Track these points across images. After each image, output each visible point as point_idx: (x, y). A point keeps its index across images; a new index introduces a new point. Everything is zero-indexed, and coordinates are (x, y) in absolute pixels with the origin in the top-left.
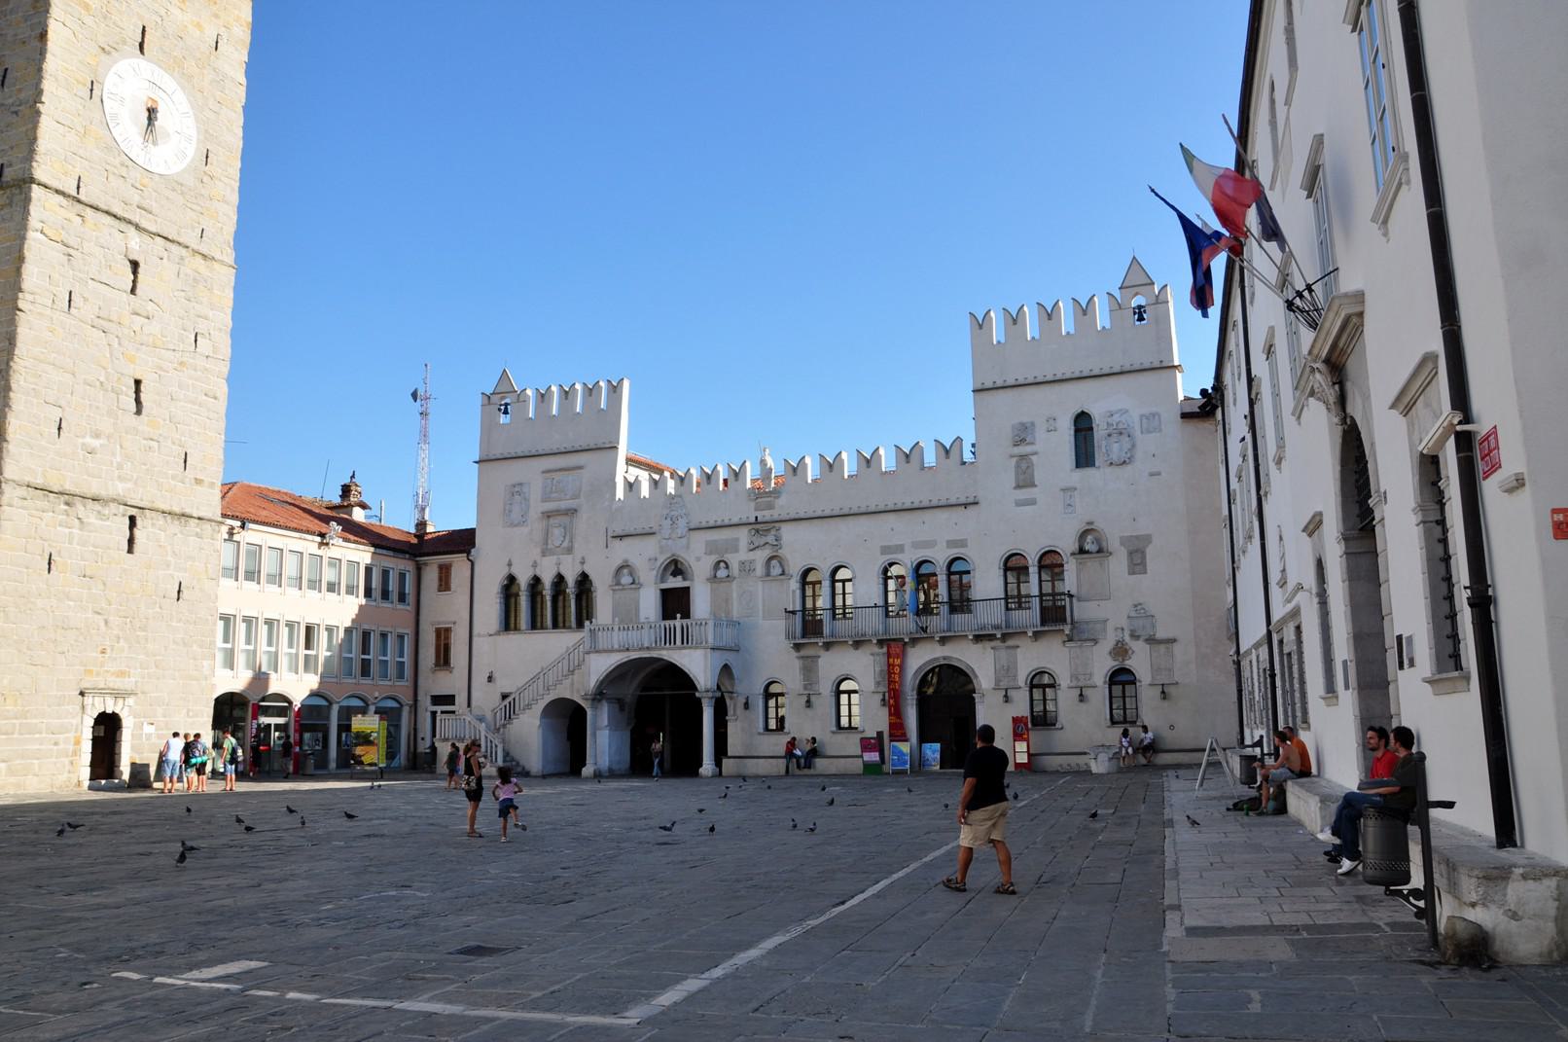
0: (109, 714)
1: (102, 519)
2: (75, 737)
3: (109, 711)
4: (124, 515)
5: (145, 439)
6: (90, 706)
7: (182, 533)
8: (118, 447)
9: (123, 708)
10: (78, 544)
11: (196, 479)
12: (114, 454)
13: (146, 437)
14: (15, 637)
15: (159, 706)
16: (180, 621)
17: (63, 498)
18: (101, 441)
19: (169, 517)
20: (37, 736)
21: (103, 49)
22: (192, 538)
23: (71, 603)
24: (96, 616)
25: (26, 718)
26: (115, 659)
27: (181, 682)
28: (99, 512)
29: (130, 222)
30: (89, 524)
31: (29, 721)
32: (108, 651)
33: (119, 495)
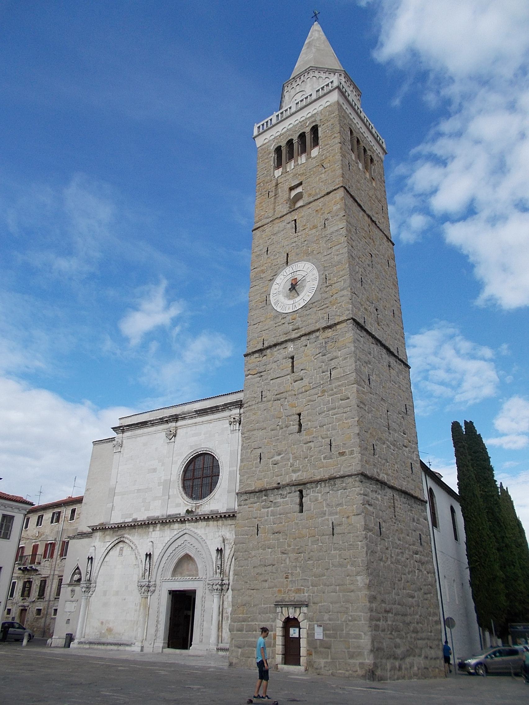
0: (291, 618)
1: (283, 498)
2: (274, 634)
3: (291, 616)
4: (295, 492)
5: (305, 444)
6: (280, 614)
7: (332, 490)
8: (291, 455)
9: (300, 614)
10: (271, 516)
11: (339, 453)
12: (289, 460)
13: (305, 441)
14: (243, 575)
15: (326, 612)
16: (335, 549)
17: (264, 493)
18: (282, 456)
19: (323, 484)
20: (254, 632)
21: (271, 280)
22: (339, 491)
23: (270, 550)
24: (285, 555)
25: (248, 622)
26: (294, 581)
27: (341, 594)
28: (281, 494)
29: (286, 341)
30: (275, 502)
31: (250, 623)
32: (290, 577)
33: (292, 481)
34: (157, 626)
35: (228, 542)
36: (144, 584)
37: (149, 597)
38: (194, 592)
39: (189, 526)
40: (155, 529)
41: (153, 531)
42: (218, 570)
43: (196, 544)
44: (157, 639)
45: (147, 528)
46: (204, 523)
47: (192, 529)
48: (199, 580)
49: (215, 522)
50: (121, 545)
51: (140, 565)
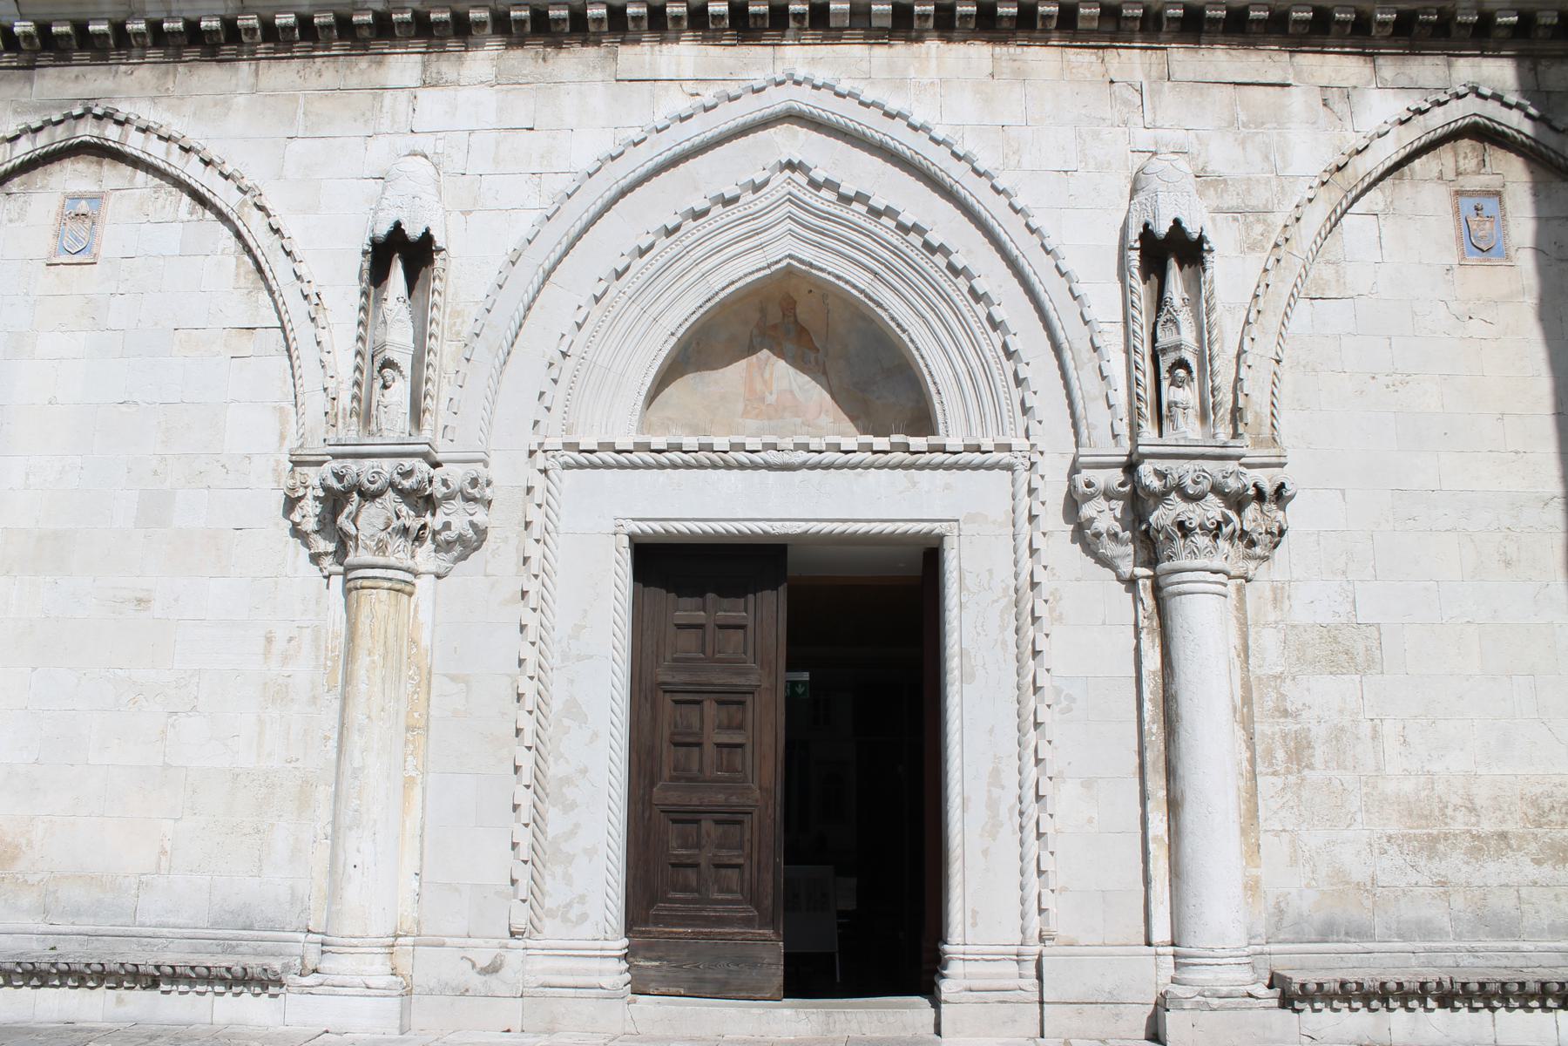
34: (537, 821)
35: (1231, 201)
36: (388, 467)
37: (424, 585)
38: (930, 555)
39: (813, 61)
40: (445, 66)
41: (425, 84)
42: (1169, 393)
43: (915, 200)
44: (549, 926)
45: (363, 63)
46: (979, 54)
47: (843, 87)
48: (974, 459)
49: (1083, 59)
50: (75, 176)
51: (302, 333)
